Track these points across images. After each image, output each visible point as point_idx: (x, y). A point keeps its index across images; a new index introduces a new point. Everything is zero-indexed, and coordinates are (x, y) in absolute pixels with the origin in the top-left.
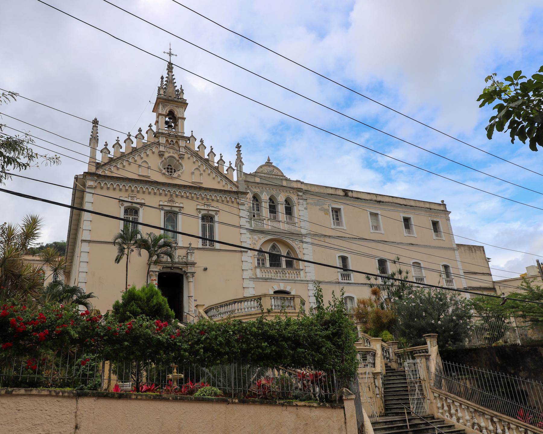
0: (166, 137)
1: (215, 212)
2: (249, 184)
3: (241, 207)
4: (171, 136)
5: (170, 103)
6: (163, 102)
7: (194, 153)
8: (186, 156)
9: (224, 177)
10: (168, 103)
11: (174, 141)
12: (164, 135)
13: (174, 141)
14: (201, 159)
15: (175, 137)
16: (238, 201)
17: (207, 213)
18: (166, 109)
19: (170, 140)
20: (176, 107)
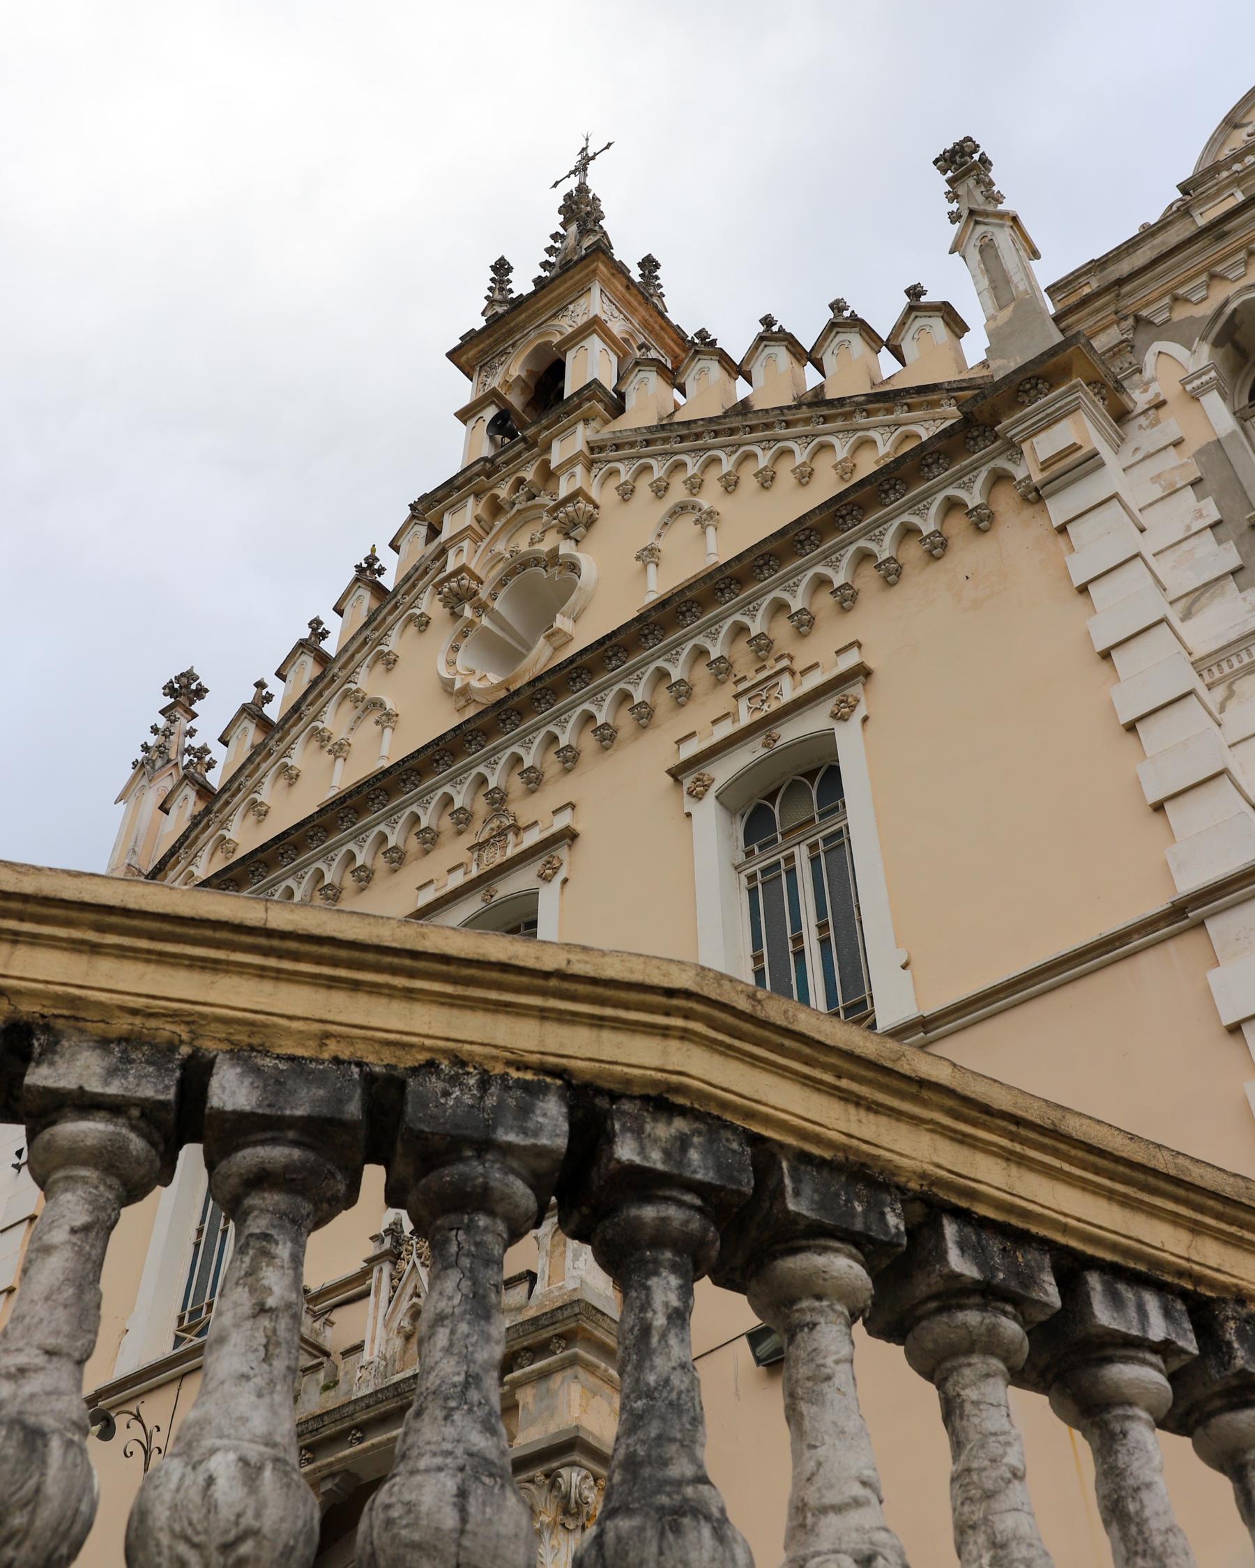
0: (477, 495)
1: (829, 705)
2: (1130, 304)
3: (1059, 508)
4: (507, 463)
5: (522, 327)
6: (484, 352)
7: (648, 443)
8: (604, 494)
9: (869, 414)
10: (511, 333)
11: (529, 474)
12: (459, 489)
13: (529, 474)
14: (698, 436)
15: (528, 449)
16: (1020, 474)
17: (761, 752)
18: (501, 370)
19: (503, 492)
20: (554, 316)
